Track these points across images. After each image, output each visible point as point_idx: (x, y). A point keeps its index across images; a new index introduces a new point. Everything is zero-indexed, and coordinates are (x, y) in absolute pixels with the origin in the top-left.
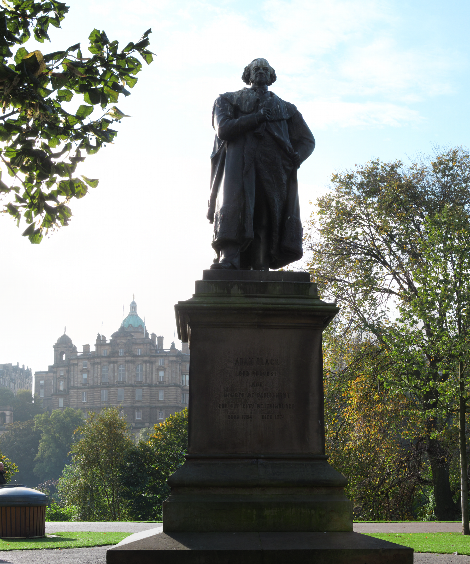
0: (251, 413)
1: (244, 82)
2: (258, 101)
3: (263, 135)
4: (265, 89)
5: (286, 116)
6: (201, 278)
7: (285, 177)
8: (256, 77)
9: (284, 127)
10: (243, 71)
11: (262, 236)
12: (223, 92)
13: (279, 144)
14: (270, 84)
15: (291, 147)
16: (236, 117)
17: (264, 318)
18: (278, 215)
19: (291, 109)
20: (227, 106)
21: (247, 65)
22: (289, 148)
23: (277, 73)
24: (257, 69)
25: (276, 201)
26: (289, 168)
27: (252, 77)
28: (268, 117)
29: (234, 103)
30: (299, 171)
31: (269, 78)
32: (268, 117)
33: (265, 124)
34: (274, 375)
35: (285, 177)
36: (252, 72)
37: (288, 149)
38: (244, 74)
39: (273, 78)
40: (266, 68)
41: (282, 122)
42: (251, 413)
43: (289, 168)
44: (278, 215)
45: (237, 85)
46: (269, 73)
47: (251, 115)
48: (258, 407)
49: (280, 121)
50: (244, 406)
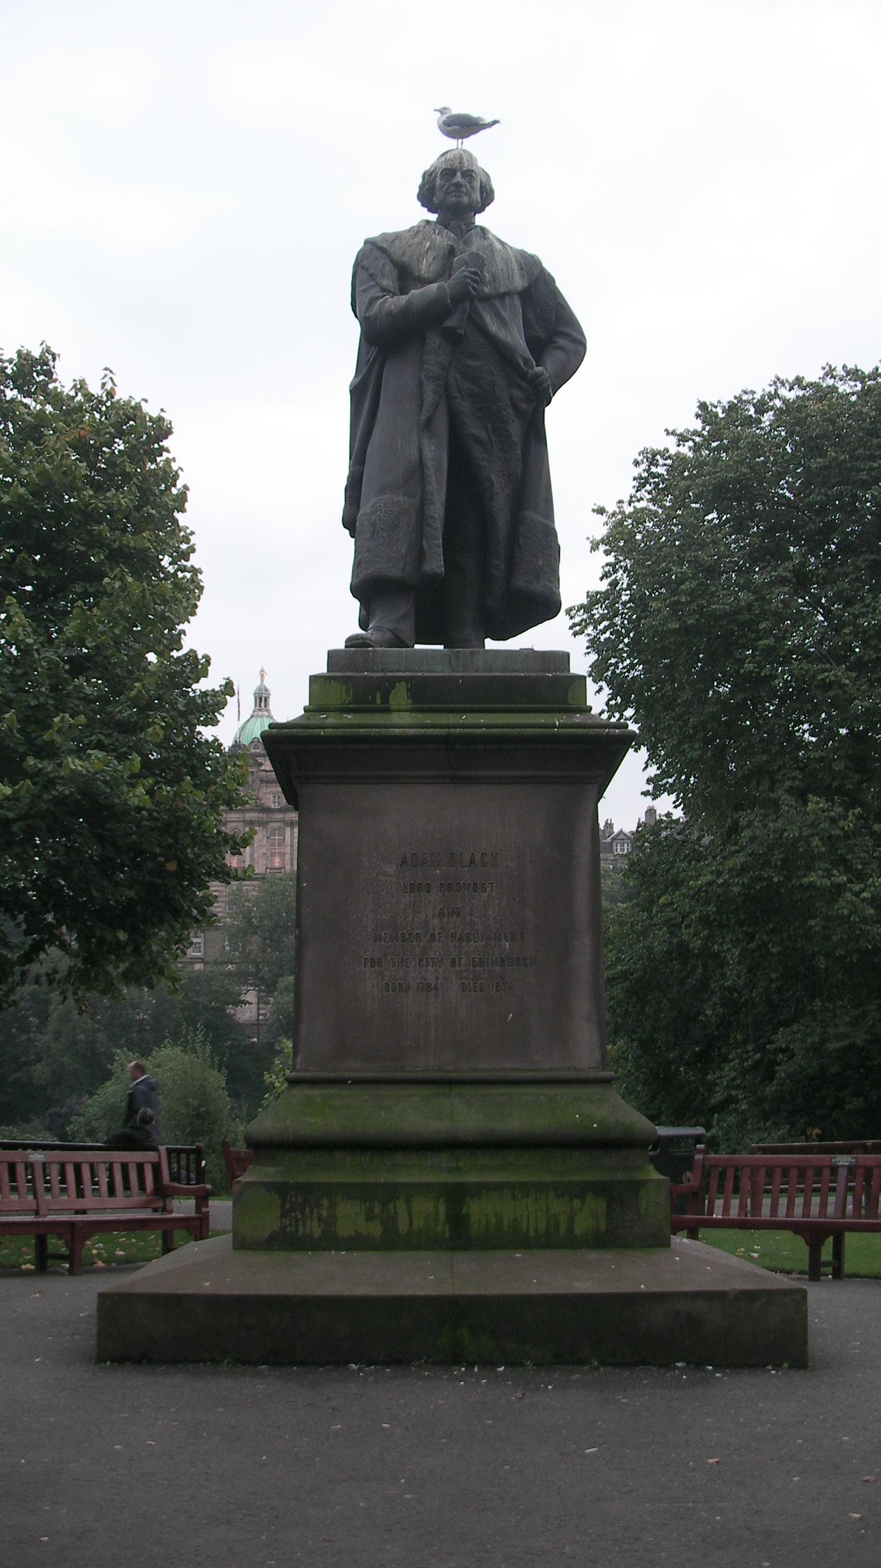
0: (437, 979)
1: (423, 205)
2: (451, 252)
3: (463, 333)
4: (471, 225)
6: (322, 668)
7: (515, 429)
8: (448, 193)
10: (419, 181)
12: (374, 233)
13: (501, 352)
14: (481, 210)
15: (529, 355)
16: (403, 291)
17: (454, 760)
18: (502, 517)
19: (531, 267)
20: (380, 268)
21: (427, 167)
25: (497, 486)
26: (524, 406)
30: (552, 414)
31: (477, 196)
33: (467, 306)
34: (488, 890)
35: (515, 429)
38: (421, 187)
39: (487, 196)
42: (437, 979)
45: (406, 213)
46: (477, 184)
48: (453, 963)
49: (502, 296)
50: (420, 962)
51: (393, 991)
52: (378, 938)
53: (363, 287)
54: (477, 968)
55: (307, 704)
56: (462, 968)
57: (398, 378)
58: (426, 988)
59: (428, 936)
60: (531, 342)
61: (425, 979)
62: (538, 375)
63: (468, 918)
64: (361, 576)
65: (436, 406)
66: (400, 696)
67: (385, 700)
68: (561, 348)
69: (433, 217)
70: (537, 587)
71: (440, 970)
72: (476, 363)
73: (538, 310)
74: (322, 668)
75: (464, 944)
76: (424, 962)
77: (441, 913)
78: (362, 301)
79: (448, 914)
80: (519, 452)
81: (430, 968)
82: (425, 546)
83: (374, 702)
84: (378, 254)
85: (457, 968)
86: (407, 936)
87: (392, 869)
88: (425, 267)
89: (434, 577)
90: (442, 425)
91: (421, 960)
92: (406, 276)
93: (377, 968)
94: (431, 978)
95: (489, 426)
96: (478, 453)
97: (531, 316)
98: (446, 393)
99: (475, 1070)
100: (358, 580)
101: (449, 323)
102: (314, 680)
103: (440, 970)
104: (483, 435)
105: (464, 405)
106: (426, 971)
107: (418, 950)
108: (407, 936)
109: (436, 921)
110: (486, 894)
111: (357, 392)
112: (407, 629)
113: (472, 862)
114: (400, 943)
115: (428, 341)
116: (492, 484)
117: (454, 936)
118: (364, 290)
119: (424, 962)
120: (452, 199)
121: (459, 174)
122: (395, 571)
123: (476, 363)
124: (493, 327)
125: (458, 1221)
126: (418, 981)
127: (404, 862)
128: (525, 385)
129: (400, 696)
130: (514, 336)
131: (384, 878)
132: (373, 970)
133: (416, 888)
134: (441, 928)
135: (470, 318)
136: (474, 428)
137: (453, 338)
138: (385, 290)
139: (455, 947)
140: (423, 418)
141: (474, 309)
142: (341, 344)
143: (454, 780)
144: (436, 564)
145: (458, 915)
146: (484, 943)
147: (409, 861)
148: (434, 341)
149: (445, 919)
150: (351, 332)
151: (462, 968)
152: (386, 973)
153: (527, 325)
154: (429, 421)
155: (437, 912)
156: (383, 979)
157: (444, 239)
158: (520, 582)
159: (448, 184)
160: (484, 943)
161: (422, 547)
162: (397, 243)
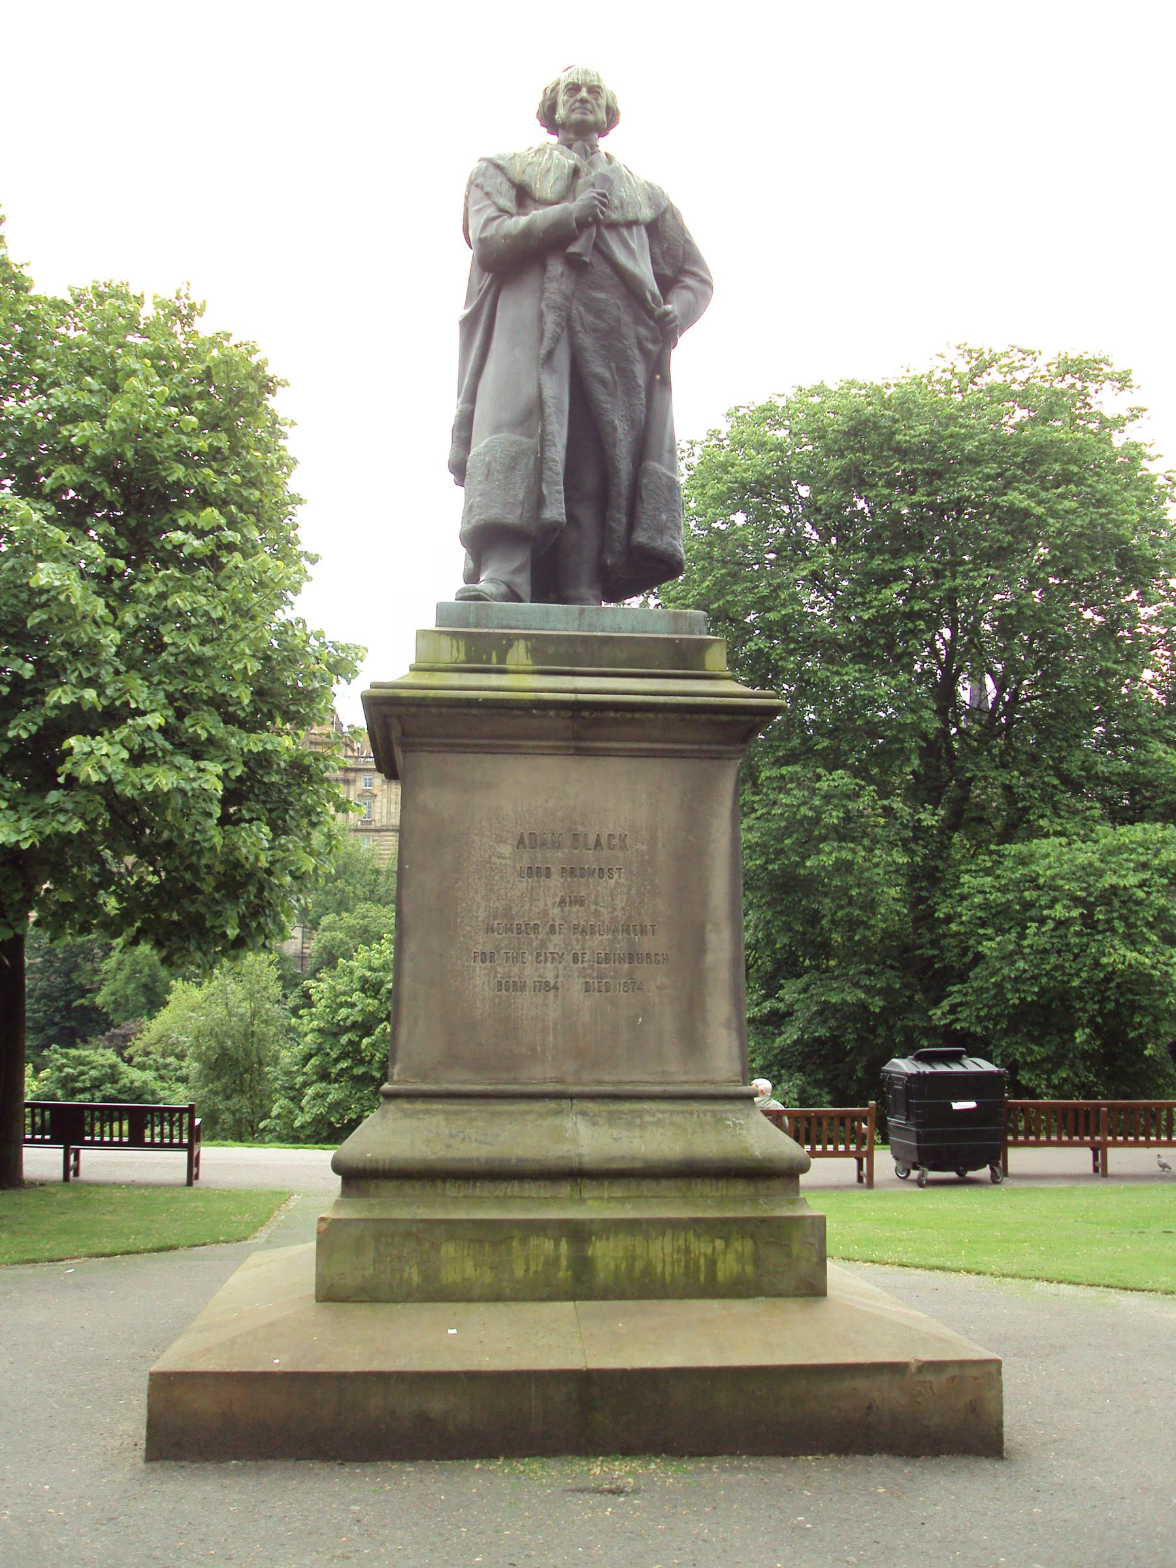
0: (557, 976)
2: (576, 172)
3: (588, 260)
4: (594, 147)
5: (646, 214)
6: (430, 624)
7: (640, 371)
9: (639, 240)
10: (540, 98)
11: (586, 515)
15: (657, 292)
18: (624, 466)
21: (549, 82)
22: (653, 294)
23: (621, 105)
24: (574, 88)
25: (620, 431)
26: (650, 346)
27: (561, 113)
28: (602, 213)
29: (518, 178)
31: (602, 116)
32: (602, 213)
34: (616, 876)
35: (640, 371)
36: (562, 98)
37: (649, 297)
38: (543, 104)
40: (599, 87)
41: (635, 229)
42: (557, 976)
43: (650, 346)
44: (624, 466)
46: (603, 102)
47: (557, 208)
48: (575, 959)
49: (631, 224)
50: (537, 957)
51: (507, 990)
52: (490, 929)
53: (477, 207)
54: (603, 965)
56: (586, 965)
57: (517, 309)
58: (544, 987)
59: (547, 928)
60: (659, 277)
62: (667, 314)
63: (593, 907)
64: (473, 522)
65: (556, 340)
66: (519, 656)
67: (502, 660)
68: (688, 287)
69: (554, 139)
70: (661, 543)
71: (561, 967)
72: (602, 296)
73: (666, 246)
74: (430, 624)
75: (588, 937)
76: (542, 958)
77: (562, 902)
78: (475, 224)
79: (571, 902)
80: (643, 396)
81: (549, 964)
82: (545, 492)
83: (489, 661)
84: (492, 170)
85: (579, 965)
86: (523, 928)
87: (507, 850)
88: (546, 188)
89: (554, 527)
90: (562, 358)
91: (538, 955)
92: (523, 195)
93: (488, 964)
94: (550, 976)
95: (613, 365)
96: (600, 395)
97: (657, 251)
98: (568, 323)
99: (600, 1082)
100: (469, 527)
101: (573, 249)
102: (422, 634)
104: (607, 375)
105: (586, 341)
107: (535, 943)
108: (523, 928)
109: (557, 910)
110: (613, 881)
111: (469, 324)
112: (523, 583)
113: (598, 844)
115: (550, 268)
116: (615, 429)
117: (576, 927)
118: (479, 211)
119: (542, 958)
120: (576, 116)
121: (584, 89)
122: (512, 517)
123: (602, 296)
124: (621, 257)
125: (582, 1266)
126: (536, 979)
127: (521, 842)
128: (652, 323)
129: (519, 656)
130: (643, 269)
131: (497, 861)
132: (483, 965)
133: (536, 872)
134: (563, 918)
135: (596, 247)
136: (598, 368)
137: (576, 265)
138: (503, 211)
139: (577, 940)
140: (543, 351)
141: (599, 235)
142: (449, 276)
143: (580, 752)
144: (556, 511)
145: (582, 904)
146: (610, 936)
147: (527, 842)
148: (556, 267)
149: (567, 909)
150: (465, 258)
151: (586, 965)
152: (500, 970)
153: (654, 262)
154: (550, 355)
155: (558, 900)
156: (495, 977)
157: (570, 159)
158: (641, 537)
159: (572, 100)
160: (610, 936)
161: (541, 493)
162: (518, 160)
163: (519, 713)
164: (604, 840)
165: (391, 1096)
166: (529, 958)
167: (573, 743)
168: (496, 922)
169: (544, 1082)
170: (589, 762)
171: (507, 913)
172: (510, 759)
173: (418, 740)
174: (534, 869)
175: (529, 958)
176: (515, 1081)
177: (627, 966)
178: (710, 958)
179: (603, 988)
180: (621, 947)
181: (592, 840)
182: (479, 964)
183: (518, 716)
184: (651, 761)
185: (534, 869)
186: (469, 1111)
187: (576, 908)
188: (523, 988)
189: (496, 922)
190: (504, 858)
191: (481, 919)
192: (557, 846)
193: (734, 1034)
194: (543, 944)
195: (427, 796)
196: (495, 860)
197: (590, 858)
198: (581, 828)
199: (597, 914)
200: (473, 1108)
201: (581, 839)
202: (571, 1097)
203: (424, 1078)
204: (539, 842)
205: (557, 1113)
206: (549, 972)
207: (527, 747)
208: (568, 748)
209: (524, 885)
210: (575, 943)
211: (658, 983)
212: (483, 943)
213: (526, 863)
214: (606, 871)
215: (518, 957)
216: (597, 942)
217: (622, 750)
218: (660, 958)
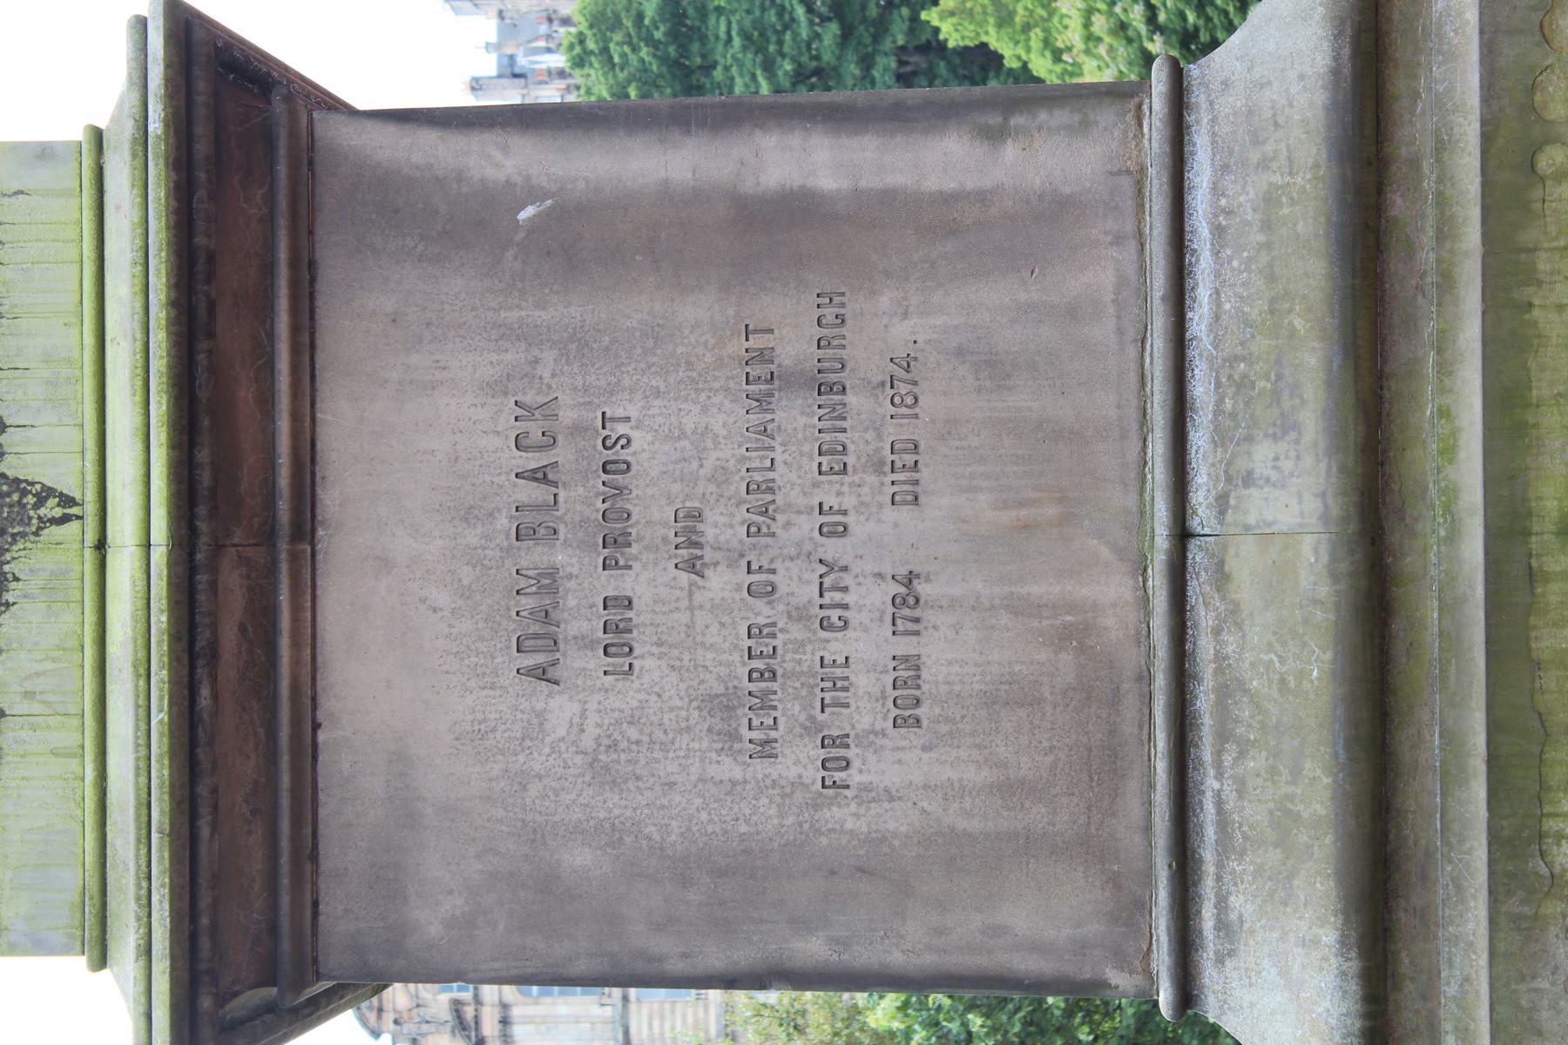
0: (880, 575)
34: (622, 429)
54: (851, 460)
55: (82, 961)
58: (907, 602)
59: (760, 604)
61: (883, 613)
76: (834, 614)
77: (693, 566)
81: (849, 598)
86: (758, 664)
87: (561, 709)
91: (824, 624)
103: (856, 568)
106: (860, 608)
107: (797, 632)
108: (758, 664)
110: (634, 434)
113: (540, 476)
114: (775, 686)
117: (753, 531)
119: (834, 614)
126: (890, 629)
127: (542, 674)
131: (592, 730)
132: (856, 764)
133: (617, 639)
134: (732, 565)
139: (788, 525)
143: (306, 525)
145: (697, 516)
147: (540, 658)
151: (849, 502)
163: (205, 692)
164: (532, 461)
165: (1187, 995)
166: (837, 647)
167: (283, 546)
168: (747, 734)
169: (1145, 601)
170: (331, 499)
171: (721, 705)
172: (329, 705)
173: (286, 945)
174: (609, 638)
175: (837, 647)
176: (1145, 678)
177: (851, 398)
178: (828, 182)
179: (909, 459)
180: (796, 415)
181: (531, 493)
182: (854, 777)
183: (215, 696)
184: (325, 340)
185: (609, 638)
186: (1219, 803)
187: (709, 533)
188: (912, 663)
189: (747, 734)
190: (583, 714)
191: (737, 773)
192: (549, 582)
193: (1018, 120)
194: (798, 615)
195: (430, 919)
196: (588, 742)
197: (580, 498)
198: (504, 523)
199: (720, 476)
200: (1211, 783)
201: (529, 518)
202: (1182, 535)
203: (1142, 907)
204: (536, 628)
205: (1222, 578)
206: (870, 597)
207: (296, 663)
208: (294, 557)
209: (648, 664)
210: (794, 531)
211: (894, 322)
212: (800, 761)
213: (596, 661)
214: (609, 455)
215: (833, 683)
216: (795, 476)
217: (295, 416)
218: (829, 313)
